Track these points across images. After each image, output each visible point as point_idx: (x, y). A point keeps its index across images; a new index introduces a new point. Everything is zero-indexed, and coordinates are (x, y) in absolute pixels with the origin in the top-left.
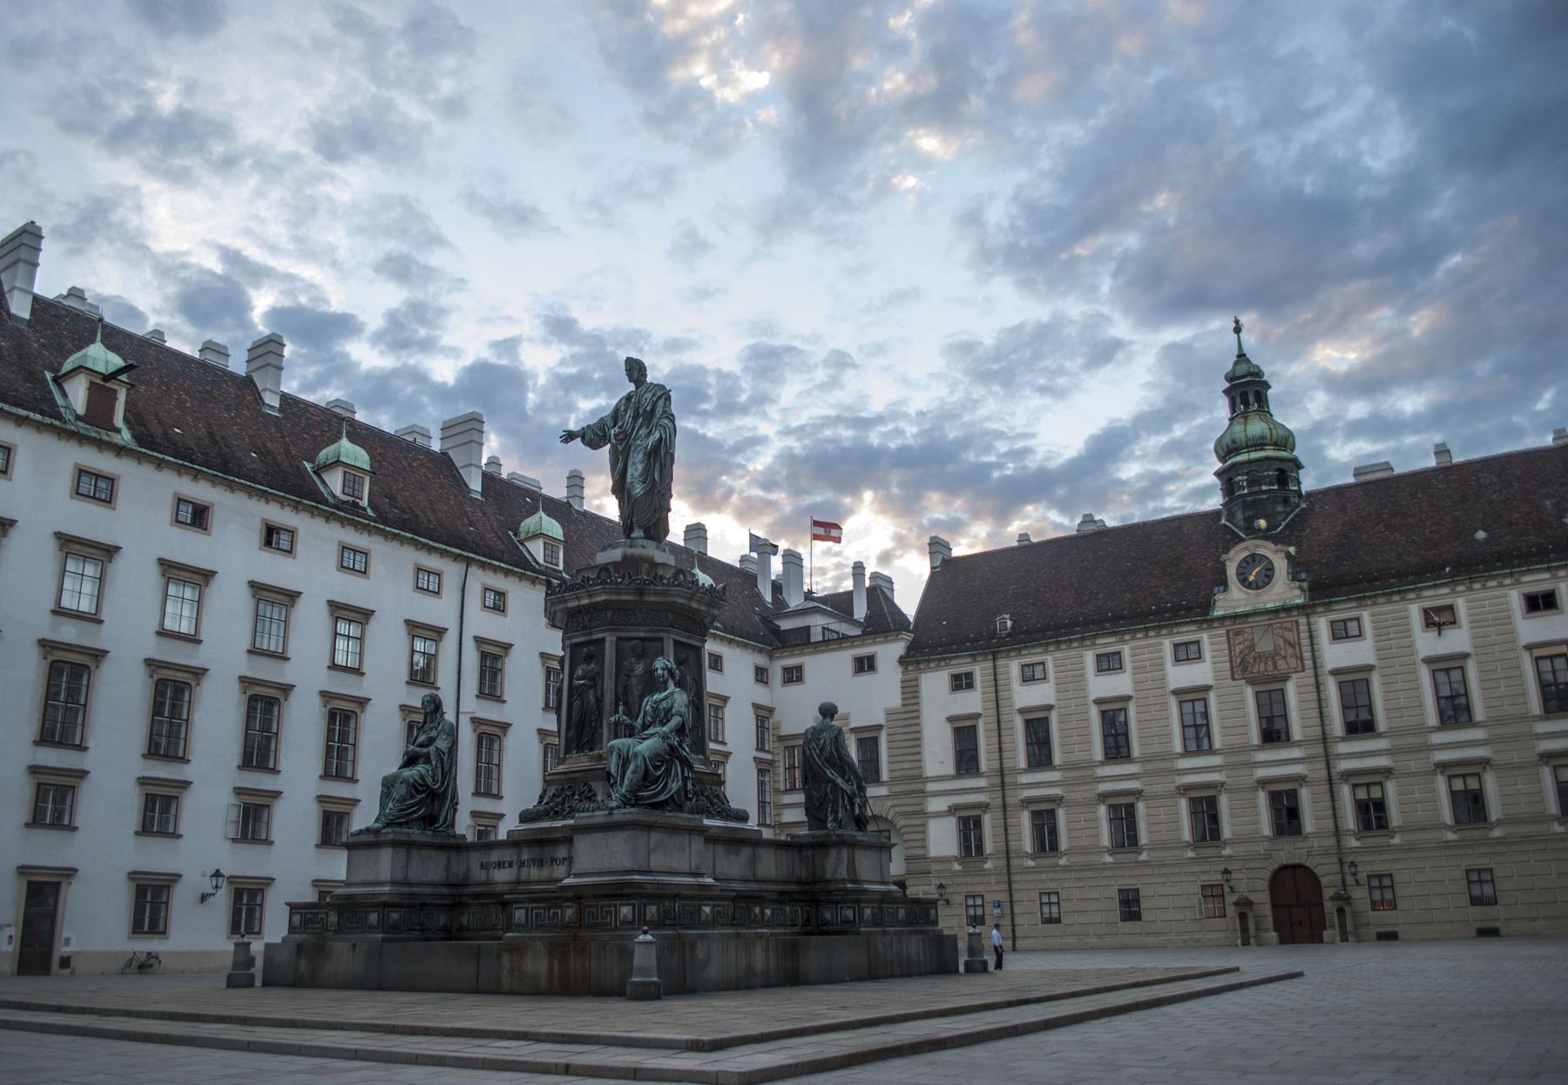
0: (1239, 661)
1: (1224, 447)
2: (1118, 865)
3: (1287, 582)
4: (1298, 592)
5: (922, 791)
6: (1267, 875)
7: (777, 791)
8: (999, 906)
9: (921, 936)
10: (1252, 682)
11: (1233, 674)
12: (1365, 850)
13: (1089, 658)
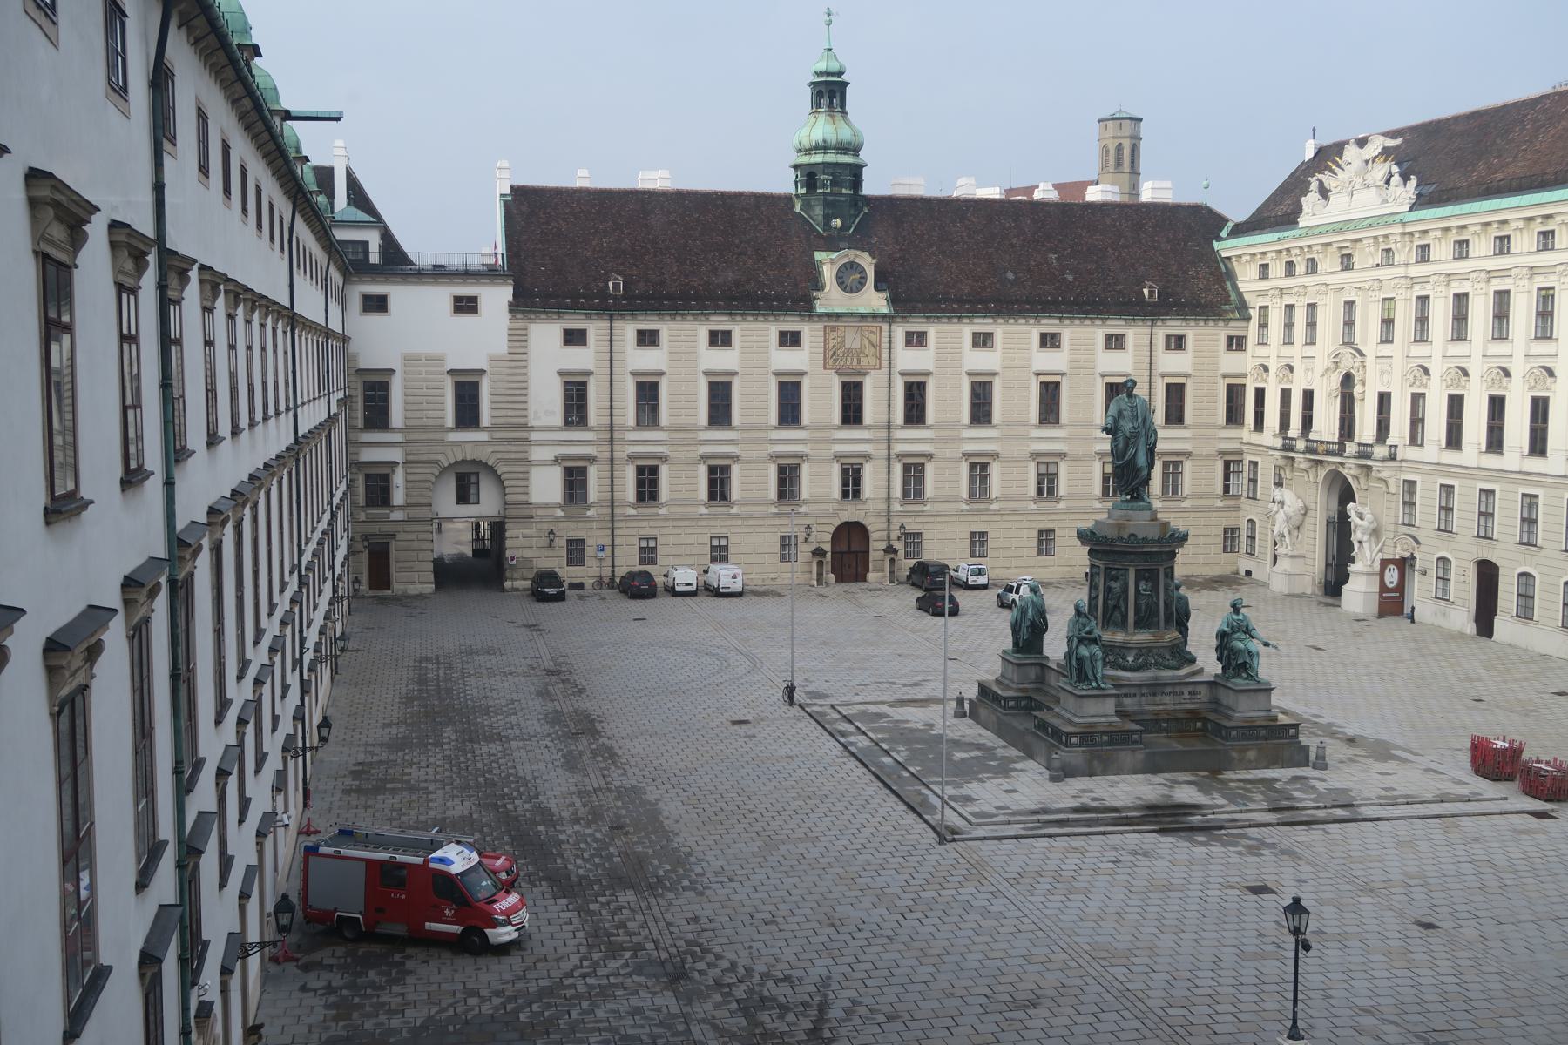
0: (831, 353)
1: (813, 144)
2: (714, 516)
5: (527, 440)
6: (832, 529)
7: (353, 428)
8: (602, 550)
10: (839, 373)
12: (905, 514)
13: (702, 331)
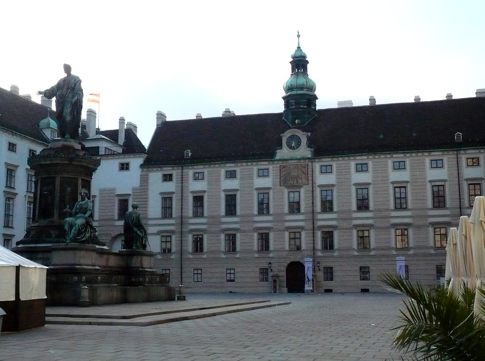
1: (287, 87)
3: (306, 147)
4: (309, 152)
9: (164, 287)
11: (280, 184)
13: (223, 171)
